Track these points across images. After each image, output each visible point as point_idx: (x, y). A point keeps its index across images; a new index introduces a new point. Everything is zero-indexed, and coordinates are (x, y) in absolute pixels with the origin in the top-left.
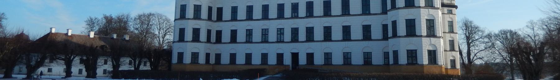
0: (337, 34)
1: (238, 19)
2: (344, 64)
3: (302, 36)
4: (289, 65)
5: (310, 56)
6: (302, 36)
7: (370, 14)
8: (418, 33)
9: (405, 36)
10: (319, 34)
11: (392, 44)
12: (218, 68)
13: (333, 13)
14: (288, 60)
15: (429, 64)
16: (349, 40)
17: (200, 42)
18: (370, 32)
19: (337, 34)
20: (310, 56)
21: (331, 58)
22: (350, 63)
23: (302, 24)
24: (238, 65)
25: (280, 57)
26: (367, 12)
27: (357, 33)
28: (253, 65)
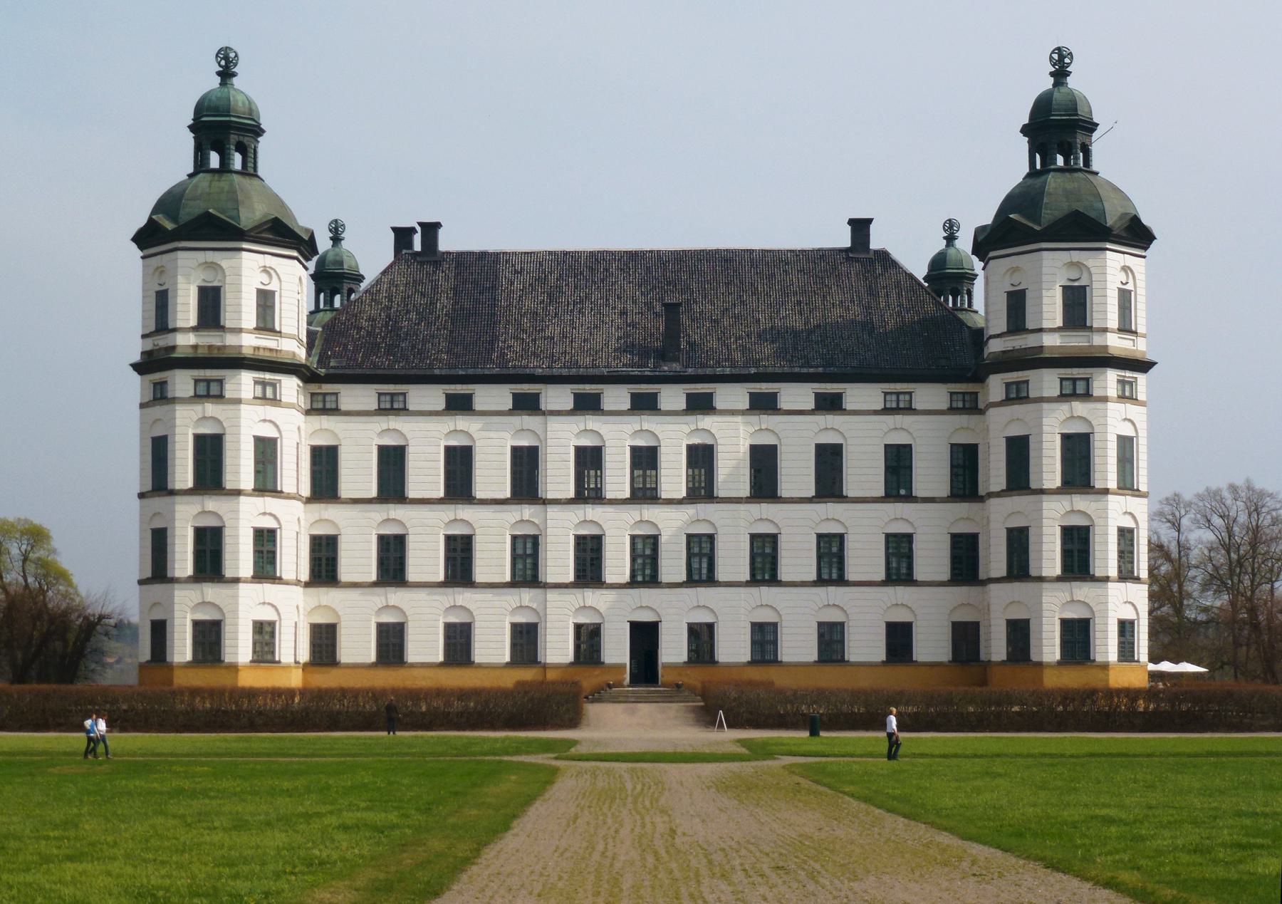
3: (673, 565)
4: (620, 667)
5: (701, 637)
6: (673, 565)
7: (910, 498)
13: (785, 490)
14: (617, 650)
15: (1119, 660)
16: (841, 581)
18: (909, 557)
20: (701, 637)
21: (775, 643)
22: (839, 658)
24: (413, 666)
28: (480, 666)
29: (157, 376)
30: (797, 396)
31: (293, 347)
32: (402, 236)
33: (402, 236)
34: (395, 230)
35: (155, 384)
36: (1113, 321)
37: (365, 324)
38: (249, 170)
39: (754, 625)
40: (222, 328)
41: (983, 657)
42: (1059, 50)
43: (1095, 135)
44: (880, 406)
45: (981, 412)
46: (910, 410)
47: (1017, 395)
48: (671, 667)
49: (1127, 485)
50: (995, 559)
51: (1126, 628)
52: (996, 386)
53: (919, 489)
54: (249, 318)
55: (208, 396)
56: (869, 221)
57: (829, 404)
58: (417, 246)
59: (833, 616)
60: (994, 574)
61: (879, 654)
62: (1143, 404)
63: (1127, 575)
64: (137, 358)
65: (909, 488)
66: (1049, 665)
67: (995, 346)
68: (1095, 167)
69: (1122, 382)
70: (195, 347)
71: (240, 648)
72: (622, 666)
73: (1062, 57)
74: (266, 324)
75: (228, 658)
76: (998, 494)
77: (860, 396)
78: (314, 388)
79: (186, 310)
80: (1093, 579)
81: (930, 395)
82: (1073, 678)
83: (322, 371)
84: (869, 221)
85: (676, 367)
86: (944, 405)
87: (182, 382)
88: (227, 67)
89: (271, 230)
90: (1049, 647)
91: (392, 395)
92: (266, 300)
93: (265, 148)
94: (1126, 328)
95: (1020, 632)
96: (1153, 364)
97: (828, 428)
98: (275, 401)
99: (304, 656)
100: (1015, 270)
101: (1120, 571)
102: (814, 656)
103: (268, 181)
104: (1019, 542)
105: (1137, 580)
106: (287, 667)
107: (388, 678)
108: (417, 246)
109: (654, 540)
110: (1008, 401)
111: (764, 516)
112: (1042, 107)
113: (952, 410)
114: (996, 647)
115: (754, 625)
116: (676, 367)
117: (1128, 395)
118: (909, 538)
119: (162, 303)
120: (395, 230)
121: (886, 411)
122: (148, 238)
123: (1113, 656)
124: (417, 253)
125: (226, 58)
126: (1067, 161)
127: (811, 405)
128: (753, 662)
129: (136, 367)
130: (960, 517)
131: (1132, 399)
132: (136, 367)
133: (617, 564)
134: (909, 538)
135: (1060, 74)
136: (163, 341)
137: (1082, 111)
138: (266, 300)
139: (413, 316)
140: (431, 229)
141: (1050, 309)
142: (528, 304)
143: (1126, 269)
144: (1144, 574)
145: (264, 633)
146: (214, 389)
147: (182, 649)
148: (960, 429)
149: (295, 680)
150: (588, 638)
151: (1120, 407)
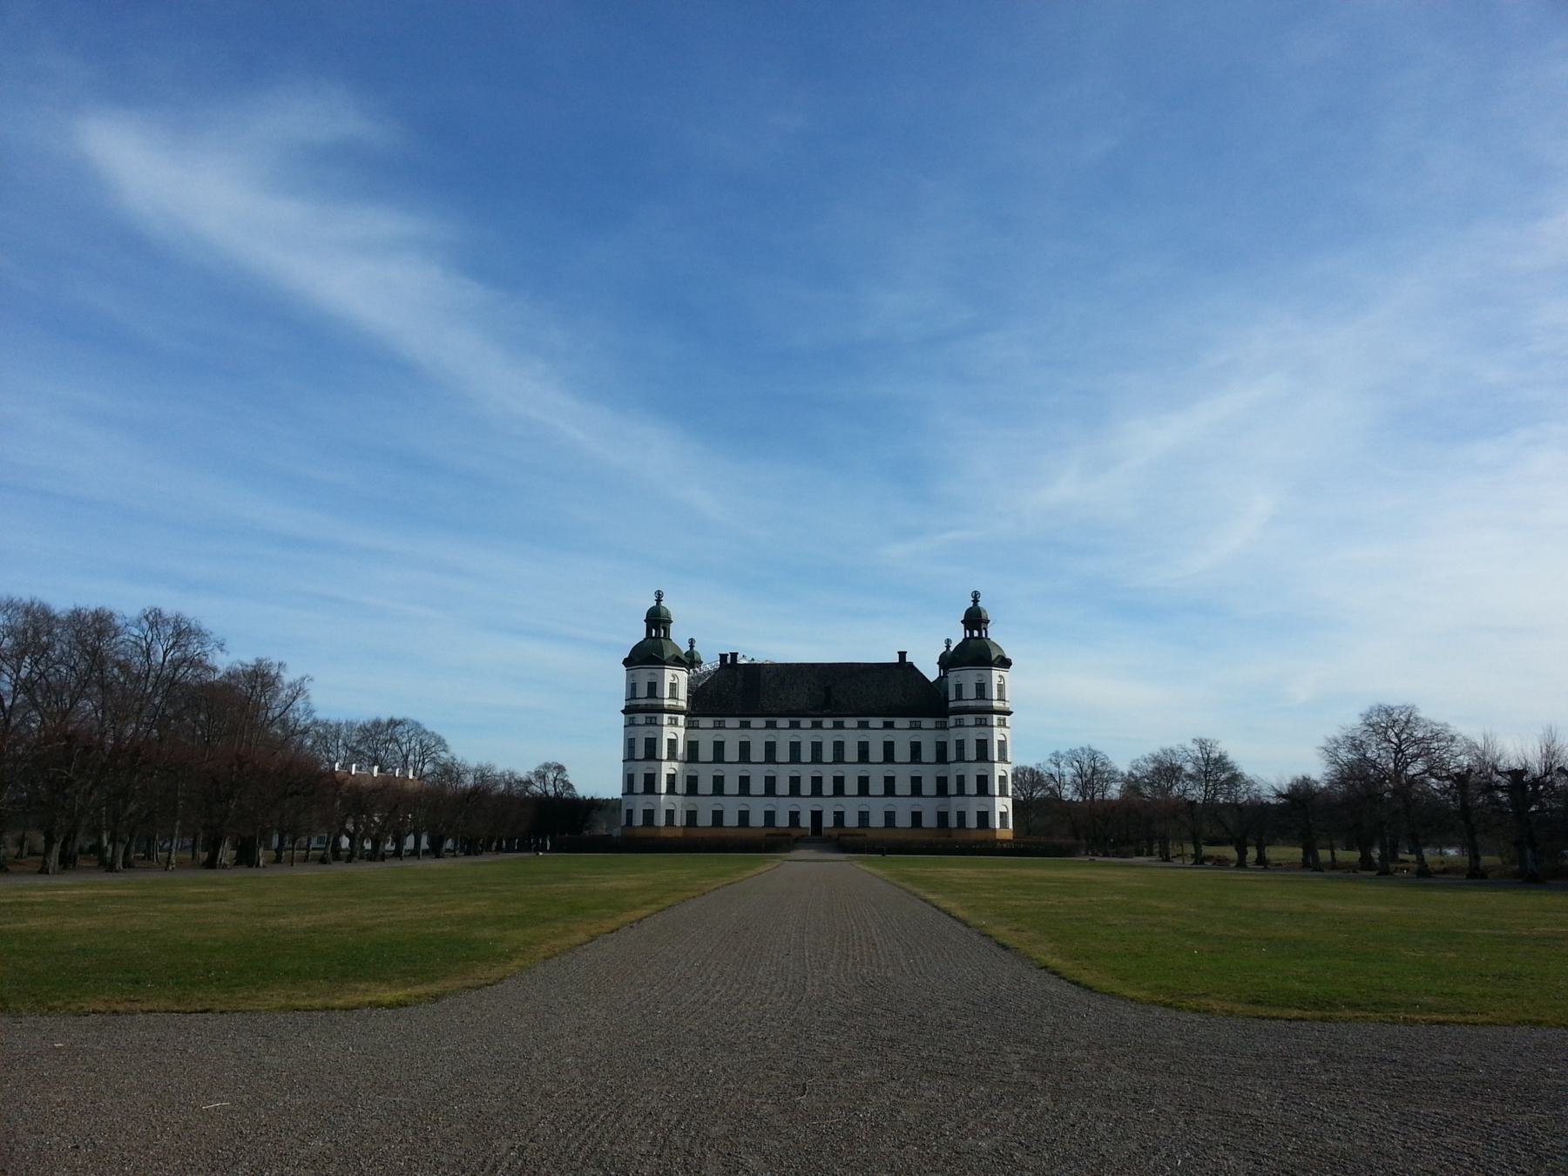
0: (877, 787)
1: (726, 760)
2: (886, 827)
3: (828, 787)
5: (839, 817)
6: (828, 787)
7: (921, 763)
8: (990, 792)
9: (976, 796)
10: (851, 786)
11: (954, 805)
12: (693, 832)
14: (806, 821)
17: (676, 794)
19: (877, 787)
20: (839, 817)
23: (828, 773)
25: (794, 816)
26: (918, 760)
27: (903, 786)
29: (631, 715)
30: (876, 722)
31: (683, 704)
32: (723, 657)
33: (723, 657)
34: (720, 655)
35: (630, 718)
36: (995, 696)
37: (708, 693)
38: (667, 636)
39: (859, 812)
40: (657, 698)
41: (949, 826)
42: (975, 592)
43: (989, 625)
44: (908, 727)
45: (948, 729)
46: (920, 728)
47: (959, 725)
48: (825, 828)
49: (1003, 759)
50: (952, 788)
51: (1003, 815)
52: (952, 720)
53: (924, 759)
54: (667, 694)
55: (651, 724)
56: (905, 652)
57: (888, 726)
58: (729, 661)
59: (890, 809)
60: (952, 793)
61: (909, 824)
62: (1009, 728)
63: (1003, 794)
64: (623, 708)
65: (920, 759)
66: (973, 829)
67: (951, 705)
68: (989, 637)
69: (999, 719)
70: (646, 705)
71: (661, 820)
72: (808, 828)
73: (976, 595)
74: (673, 696)
75: (656, 824)
76: (954, 762)
77: (901, 722)
78: (689, 718)
79: (643, 691)
80: (990, 796)
81: (928, 722)
82: (982, 834)
83: (693, 712)
84: (905, 652)
85: (829, 711)
86: (934, 726)
87: (640, 718)
88: (659, 597)
89: (675, 661)
90: (972, 822)
91: (720, 721)
92: (673, 687)
93: (672, 627)
94: (1001, 699)
95: (961, 816)
96: (1011, 713)
97: (889, 735)
98: (676, 724)
99: (684, 823)
100: (958, 676)
101: (1000, 792)
102: (883, 825)
103: (673, 641)
104: (961, 780)
105: (1007, 796)
106: (678, 827)
107: (717, 832)
108: (729, 661)
109: (820, 779)
110: (956, 726)
111: (863, 770)
112: (969, 612)
113: (936, 728)
114: (953, 822)
115: (859, 812)
116: (829, 711)
117: (1003, 724)
118: (920, 778)
119: (632, 689)
120: (720, 655)
121: (911, 728)
122: (627, 662)
123: (998, 826)
124: (728, 665)
125: (659, 594)
126: (980, 633)
127: (881, 726)
128: (859, 827)
129: (623, 711)
130: (940, 770)
131: (1004, 726)
132: (623, 711)
133: (806, 787)
134: (920, 778)
135: (976, 601)
136: (634, 702)
137: (983, 615)
138: (673, 687)
139: (727, 690)
140: (734, 655)
141: (970, 692)
142: (772, 685)
143: (1001, 676)
144: (1010, 794)
145: (670, 814)
146: (653, 721)
147: (638, 820)
148: (941, 736)
149: (680, 833)
150: (794, 816)
151: (999, 729)
